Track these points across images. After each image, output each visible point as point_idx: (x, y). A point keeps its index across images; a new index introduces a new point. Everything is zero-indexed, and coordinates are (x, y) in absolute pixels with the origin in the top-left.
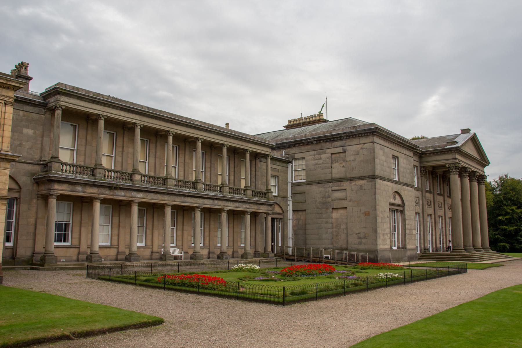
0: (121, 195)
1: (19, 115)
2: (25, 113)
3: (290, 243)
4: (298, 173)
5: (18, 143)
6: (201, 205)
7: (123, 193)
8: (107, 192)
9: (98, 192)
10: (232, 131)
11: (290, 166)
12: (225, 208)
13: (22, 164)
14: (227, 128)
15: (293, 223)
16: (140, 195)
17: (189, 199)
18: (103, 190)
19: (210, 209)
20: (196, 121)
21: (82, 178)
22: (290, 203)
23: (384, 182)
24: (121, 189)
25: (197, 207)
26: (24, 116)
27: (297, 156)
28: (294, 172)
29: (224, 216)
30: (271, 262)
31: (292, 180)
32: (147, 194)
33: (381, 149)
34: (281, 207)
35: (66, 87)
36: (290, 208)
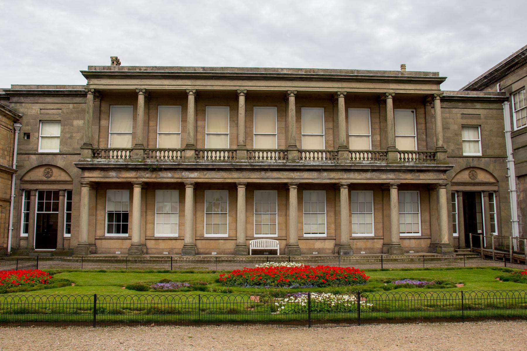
1: (69, 108)
2: (75, 105)
3: (516, 231)
4: (520, 115)
5: (68, 135)
6: (296, 181)
7: (169, 175)
8: (147, 175)
9: (136, 176)
10: (411, 73)
11: (506, 106)
12: (344, 182)
13: (73, 156)
14: (403, 70)
15: (518, 196)
16: (195, 175)
17: (275, 174)
18: (143, 174)
20: (282, 69)
21: (117, 162)
22: (511, 166)
24: (166, 169)
25: (292, 184)
26: (74, 108)
27: (515, 87)
28: (514, 115)
30: (439, 259)
31: (512, 127)
32: (205, 172)
34: (491, 174)
35: (95, 69)
36: (512, 173)
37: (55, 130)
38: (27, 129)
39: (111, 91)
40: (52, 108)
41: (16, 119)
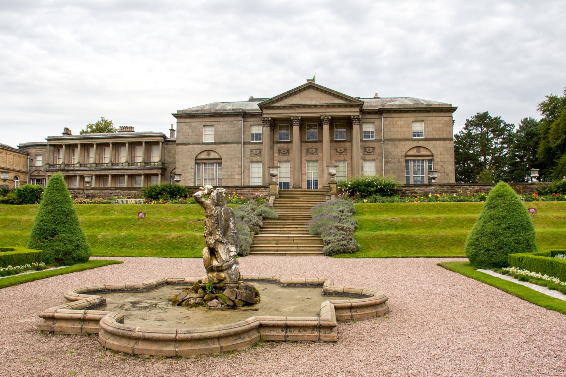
12: (126, 174)
17: (104, 171)
19: (131, 174)
23: (188, 146)
29: (110, 178)
33: (186, 125)
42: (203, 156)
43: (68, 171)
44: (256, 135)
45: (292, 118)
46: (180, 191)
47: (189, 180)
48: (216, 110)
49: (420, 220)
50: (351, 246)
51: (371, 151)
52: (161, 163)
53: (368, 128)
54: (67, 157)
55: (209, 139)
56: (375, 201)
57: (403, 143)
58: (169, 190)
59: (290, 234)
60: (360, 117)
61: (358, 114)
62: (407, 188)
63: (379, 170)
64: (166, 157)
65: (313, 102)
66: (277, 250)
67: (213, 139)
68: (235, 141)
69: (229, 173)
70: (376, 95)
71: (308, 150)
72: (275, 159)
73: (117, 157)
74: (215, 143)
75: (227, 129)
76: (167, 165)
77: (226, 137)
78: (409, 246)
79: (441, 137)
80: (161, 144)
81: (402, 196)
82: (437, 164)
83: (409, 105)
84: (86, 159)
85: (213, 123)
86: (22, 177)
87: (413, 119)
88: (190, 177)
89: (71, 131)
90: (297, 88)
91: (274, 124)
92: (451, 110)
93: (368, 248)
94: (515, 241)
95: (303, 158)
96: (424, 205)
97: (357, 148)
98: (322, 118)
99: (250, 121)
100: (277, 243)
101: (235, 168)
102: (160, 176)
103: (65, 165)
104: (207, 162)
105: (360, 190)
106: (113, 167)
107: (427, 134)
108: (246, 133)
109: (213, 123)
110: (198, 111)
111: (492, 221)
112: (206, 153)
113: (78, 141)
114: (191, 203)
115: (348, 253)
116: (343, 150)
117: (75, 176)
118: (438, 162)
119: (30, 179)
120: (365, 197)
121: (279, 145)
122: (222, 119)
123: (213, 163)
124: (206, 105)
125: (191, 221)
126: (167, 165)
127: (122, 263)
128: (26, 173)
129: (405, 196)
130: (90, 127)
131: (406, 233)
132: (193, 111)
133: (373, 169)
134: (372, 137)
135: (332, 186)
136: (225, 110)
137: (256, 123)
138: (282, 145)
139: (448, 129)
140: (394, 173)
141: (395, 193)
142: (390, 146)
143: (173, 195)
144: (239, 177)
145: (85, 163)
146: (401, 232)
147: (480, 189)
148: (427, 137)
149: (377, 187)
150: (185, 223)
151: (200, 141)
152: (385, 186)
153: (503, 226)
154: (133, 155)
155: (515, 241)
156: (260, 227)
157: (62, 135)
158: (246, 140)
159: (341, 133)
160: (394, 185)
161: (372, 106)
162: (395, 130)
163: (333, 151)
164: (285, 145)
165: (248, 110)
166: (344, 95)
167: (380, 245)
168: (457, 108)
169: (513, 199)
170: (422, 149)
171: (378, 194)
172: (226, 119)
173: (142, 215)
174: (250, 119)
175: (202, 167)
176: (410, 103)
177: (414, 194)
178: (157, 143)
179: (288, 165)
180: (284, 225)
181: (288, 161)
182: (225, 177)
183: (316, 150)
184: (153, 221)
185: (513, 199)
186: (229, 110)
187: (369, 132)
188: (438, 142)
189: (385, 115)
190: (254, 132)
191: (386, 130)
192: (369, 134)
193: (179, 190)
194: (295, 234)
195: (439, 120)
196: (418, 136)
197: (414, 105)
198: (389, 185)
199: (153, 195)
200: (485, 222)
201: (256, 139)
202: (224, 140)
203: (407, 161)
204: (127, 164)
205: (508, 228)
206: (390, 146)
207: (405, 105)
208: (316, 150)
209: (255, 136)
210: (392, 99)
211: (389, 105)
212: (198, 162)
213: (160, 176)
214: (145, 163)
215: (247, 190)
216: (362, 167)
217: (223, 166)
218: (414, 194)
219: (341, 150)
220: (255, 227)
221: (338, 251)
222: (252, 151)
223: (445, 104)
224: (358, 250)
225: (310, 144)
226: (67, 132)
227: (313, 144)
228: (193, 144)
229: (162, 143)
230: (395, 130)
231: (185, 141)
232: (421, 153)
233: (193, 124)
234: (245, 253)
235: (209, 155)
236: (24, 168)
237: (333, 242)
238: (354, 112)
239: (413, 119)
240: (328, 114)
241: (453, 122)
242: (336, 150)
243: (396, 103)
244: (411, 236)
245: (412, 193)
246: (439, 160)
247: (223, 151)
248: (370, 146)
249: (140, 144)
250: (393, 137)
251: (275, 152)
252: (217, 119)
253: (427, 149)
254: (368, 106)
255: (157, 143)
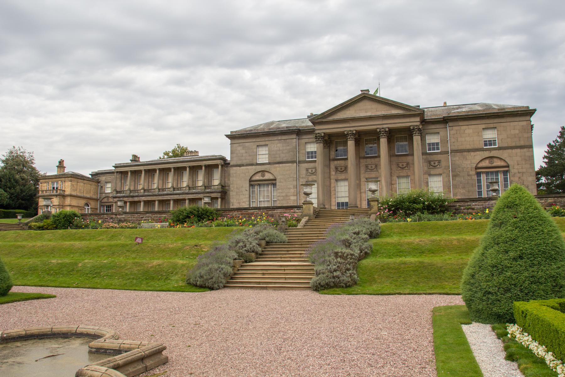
0: (136, 199)
16: (143, 198)
17: (166, 196)
23: (242, 168)
33: (240, 146)
37: (109, 185)
38: (102, 185)
39: (121, 172)
40: (108, 178)
41: (98, 182)
42: (257, 177)
43: (133, 197)
44: (312, 152)
45: (346, 133)
46: (208, 214)
47: (244, 202)
48: (270, 129)
49: (455, 242)
50: (345, 278)
51: (436, 164)
52: (220, 187)
53: (431, 139)
54: (133, 183)
55: (263, 160)
56: (420, 219)
57: (472, 154)
58: (196, 213)
59: (290, 261)
60: (421, 127)
61: (418, 123)
62: (462, 204)
63: (447, 186)
64: (226, 180)
65: (369, 114)
66: (259, 283)
67: (267, 159)
68: (289, 159)
69: (284, 194)
70: (445, 103)
71: (367, 166)
72: (332, 177)
73: (179, 182)
74: (269, 164)
75: (281, 148)
76: (227, 188)
77: (280, 157)
78: (426, 277)
79: (518, 145)
80: (220, 167)
81: (454, 213)
82: (514, 176)
83: (478, 110)
84: (150, 184)
85: (267, 143)
86: (92, 204)
87: (484, 126)
88: (244, 200)
89: (139, 158)
90: (351, 100)
91: (330, 141)
92: (528, 113)
93: (372, 281)
94: (532, 279)
95: (362, 176)
96: (469, 223)
97: (419, 162)
98: (378, 130)
99: (305, 138)
100: (263, 274)
101: (290, 188)
102: (219, 200)
103: (131, 191)
104: (262, 183)
105: (401, 208)
106: (175, 192)
107: (500, 142)
108: (301, 152)
109: (267, 143)
110: (251, 130)
111: (496, 247)
112: (260, 174)
113: (142, 167)
114: (216, 226)
115: (340, 287)
116: (405, 165)
117: (140, 202)
118: (515, 173)
119: (101, 206)
120: (408, 215)
121: (336, 162)
122: (276, 138)
123: (268, 185)
124: (261, 125)
125: (188, 247)
126: (227, 188)
127: (55, 297)
128: (97, 200)
129: (460, 213)
130: (166, 154)
131: (426, 259)
132: (247, 131)
133: (441, 184)
134: (438, 149)
135: (372, 203)
136: (279, 128)
137: (311, 140)
138: (339, 162)
139: (526, 135)
140: (464, 188)
141: (447, 210)
142: (457, 158)
143: (201, 218)
144: (295, 198)
145: (150, 188)
146: (420, 259)
147: (555, 202)
148: (501, 146)
149: (424, 203)
150: (180, 249)
151: (254, 162)
152: (433, 201)
153: (512, 254)
154: (194, 179)
155: (532, 279)
156: (257, 253)
157: (130, 162)
158: (302, 159)
159: (402, 146)
160: (444, 201)
161: (436, 115)
162: (463, 139)
163: (394, 167)
164: (342, 162)
165: (303, 127)
166: (401, 104)
167: (387, 277)
168: (535, 110)
169: (530, 210)
170: (495, 160)
171: (426, 212)
172: (280, 138)
173: (139, 240)
174: (304, 137)
175: (257, 188)
176: (480, 108)
177: (470, 211)
178: (216, 166)
179: (346, 183)
180: (288, 251)
181: (346, 179)
182: (280, 198)
183: (376, 166)
184: (148, 247)
185: (530, 210)
186: (283, 128)
187: (433, 144)
188: (514, 151)
189: (451, 124)
190: (309, 150)
191: (453, 140)
192: (434, 146)
193: (207, 212)
194: (295, 261)
195: (514, 126)
196: (490, 145)
197: (484, 110)
198: (438, 200)
199: (181, 219)
200: (486, 248)
201: (312, 157)
202: (278, 160)
203: (479, 174)
204: (188, 188)
205: (521, 257)
206: (458, 158)
207: (473, 111)
208: (376, 166)
209: (312, 154)
210: (459, 107)
211: (454, 112)
212: (252, 183)
213: (219, 200)
214: (205, 187)
215: (279, 211)
216: (427, 183)
217: (277, 187)
218: (470, 211)
219: (403, 165)
220: (249, 253)
221: (327, 284)
222: (307, 170)
223: (520, 107)
224: (355, 283)
225: (368, 160)
226: (135, 158)
227: (373, 160)
228: (247, 165)
229: (222, 166)
230: (463, 139)
231: (239, 163)
232: (495, 164)
233: (247, 144)
234: (216, 286)
235: (263, 176)
236: (94, 195)
237: (323, 273)
238: (414, 122)
239: (484, 126)
240: (385, 126)
241: (532, 126)
242: (398, 165)
243: (464, 110)
244: (431, 265)
245: (468, 209)
246: (516, 171)
247: (277, 171)
248: (435, 159)
249: (200, 167)
250: (461, 147)
251: (331, 170)
252: (271, 138)
253: (501, 159)
254: (431, 115)
255: (216, 166)
